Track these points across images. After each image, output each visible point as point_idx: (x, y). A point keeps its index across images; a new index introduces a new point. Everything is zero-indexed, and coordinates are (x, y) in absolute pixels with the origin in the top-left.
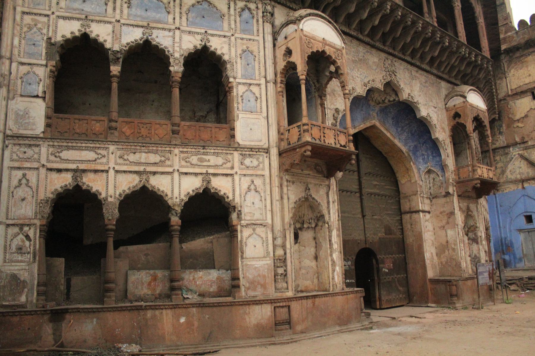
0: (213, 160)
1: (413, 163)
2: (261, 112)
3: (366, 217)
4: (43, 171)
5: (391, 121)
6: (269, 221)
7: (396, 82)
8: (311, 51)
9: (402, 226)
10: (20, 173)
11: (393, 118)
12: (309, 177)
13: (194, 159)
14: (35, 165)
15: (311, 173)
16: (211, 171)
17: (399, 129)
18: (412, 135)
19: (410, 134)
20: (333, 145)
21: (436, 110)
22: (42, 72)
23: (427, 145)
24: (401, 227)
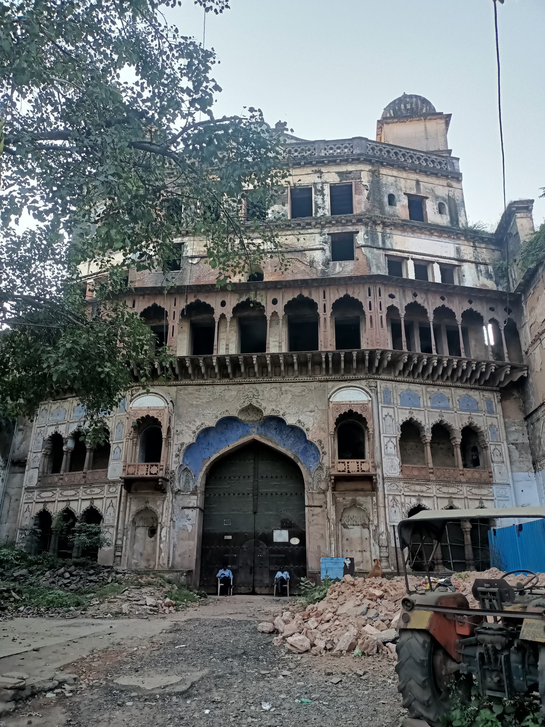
0: (97, 490)
1: (301, 463)
3: (258, 513)
4: (34, 503)
5: (274, 432)
6: (115, 524)
10: (26, 505)
11: (275, 429)
13: (88, 491)
14: (31, 501)
16: (94, 497)
17: (284, 437)
18: (299, 438)
20: (145, 476)
21: (313, 414)
22: (40, 455)
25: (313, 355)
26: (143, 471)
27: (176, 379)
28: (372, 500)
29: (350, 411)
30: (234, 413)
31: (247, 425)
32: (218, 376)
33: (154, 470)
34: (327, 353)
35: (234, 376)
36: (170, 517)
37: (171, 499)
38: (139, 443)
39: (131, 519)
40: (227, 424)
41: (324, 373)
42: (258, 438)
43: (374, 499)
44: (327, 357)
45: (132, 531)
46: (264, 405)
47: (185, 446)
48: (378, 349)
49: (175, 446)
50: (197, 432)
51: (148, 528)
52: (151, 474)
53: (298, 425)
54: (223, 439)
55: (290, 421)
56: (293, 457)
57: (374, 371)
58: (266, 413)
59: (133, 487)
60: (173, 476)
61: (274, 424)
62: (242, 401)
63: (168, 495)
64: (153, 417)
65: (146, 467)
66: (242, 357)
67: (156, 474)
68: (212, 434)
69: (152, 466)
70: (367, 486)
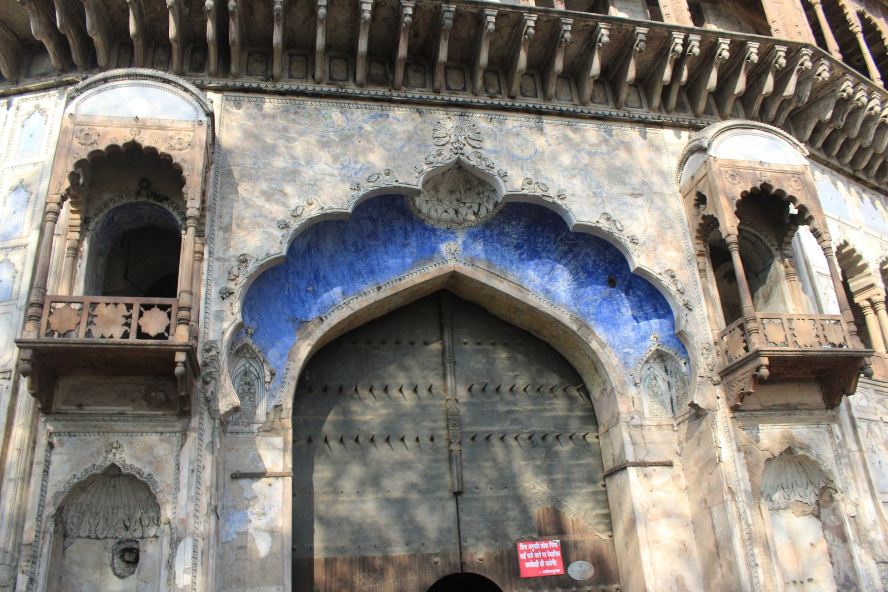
2: (18, 298)
3: (465, 496)
7: (474, 162)
8: (90, 149)
9: (608, 507)
11: (518, 247)
12: (119, 420)
15: (129, 409)
18: (590, 274)
19: (583, 276)
23: (639, 293)
24: (605, 511)
25: (649, 38)
26: (112, 323)
27: (224, 68)
28: (831, 432)
29: (766, 187)
30: (410, 178)
31: (434, 231)
32: (360, 75)
33: (154, 322)
34: (688, 31)
35: (406, 83)
36: (205, 500)
37: (207, 438)
38: (85, 246)
39: (50, 510)
40: (374, 221)
41: (657, 101)
42: (466, 270)
43: (836, 428)
44: (686, 43)
45: (54, 554)
46: (500, 165)
47: (252, 267)
48: (807, 46)
49: (216, 264)
50: (295, 225)
51: (111, 543)
52: (141, 335)
53: (604, 225)
54: (360, 266)
55: (582, 212)
56: (574, 327)
57: (773, 112)
58: (505, 190)
59: (59, 396)
60: (215, 359)
61: (515, 232)
62: (434, 150)
63: (195, 422)
64: (152, 151)
65: (123, 310)
66: (453, 8)
67: (160, 336)
68: (329, 245)
69: (148, 307)
70: (814, 397)
